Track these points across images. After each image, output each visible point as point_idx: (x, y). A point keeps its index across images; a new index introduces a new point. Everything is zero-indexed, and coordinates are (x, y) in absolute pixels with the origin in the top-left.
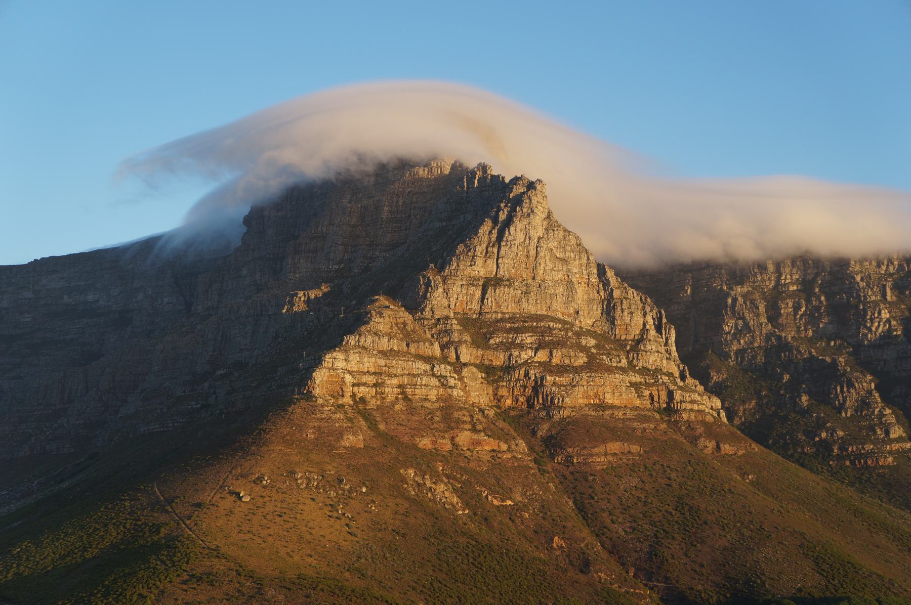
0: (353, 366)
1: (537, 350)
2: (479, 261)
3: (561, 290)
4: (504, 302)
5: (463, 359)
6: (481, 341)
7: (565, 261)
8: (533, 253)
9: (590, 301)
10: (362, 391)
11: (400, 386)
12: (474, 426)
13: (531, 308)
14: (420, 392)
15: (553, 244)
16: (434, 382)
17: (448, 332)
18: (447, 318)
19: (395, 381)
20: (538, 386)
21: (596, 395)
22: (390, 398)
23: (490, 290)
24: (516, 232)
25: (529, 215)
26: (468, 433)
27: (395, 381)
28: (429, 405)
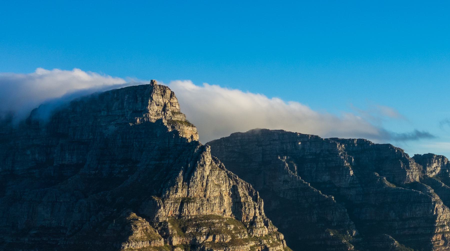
2: (180, 190)
3: (217, 200)
4: (191, 211)
7: (219, 186)
8: (205, 184)
13: (206, 212)
17: (166, 230)
18: (165, 222)
24: (198, 174)
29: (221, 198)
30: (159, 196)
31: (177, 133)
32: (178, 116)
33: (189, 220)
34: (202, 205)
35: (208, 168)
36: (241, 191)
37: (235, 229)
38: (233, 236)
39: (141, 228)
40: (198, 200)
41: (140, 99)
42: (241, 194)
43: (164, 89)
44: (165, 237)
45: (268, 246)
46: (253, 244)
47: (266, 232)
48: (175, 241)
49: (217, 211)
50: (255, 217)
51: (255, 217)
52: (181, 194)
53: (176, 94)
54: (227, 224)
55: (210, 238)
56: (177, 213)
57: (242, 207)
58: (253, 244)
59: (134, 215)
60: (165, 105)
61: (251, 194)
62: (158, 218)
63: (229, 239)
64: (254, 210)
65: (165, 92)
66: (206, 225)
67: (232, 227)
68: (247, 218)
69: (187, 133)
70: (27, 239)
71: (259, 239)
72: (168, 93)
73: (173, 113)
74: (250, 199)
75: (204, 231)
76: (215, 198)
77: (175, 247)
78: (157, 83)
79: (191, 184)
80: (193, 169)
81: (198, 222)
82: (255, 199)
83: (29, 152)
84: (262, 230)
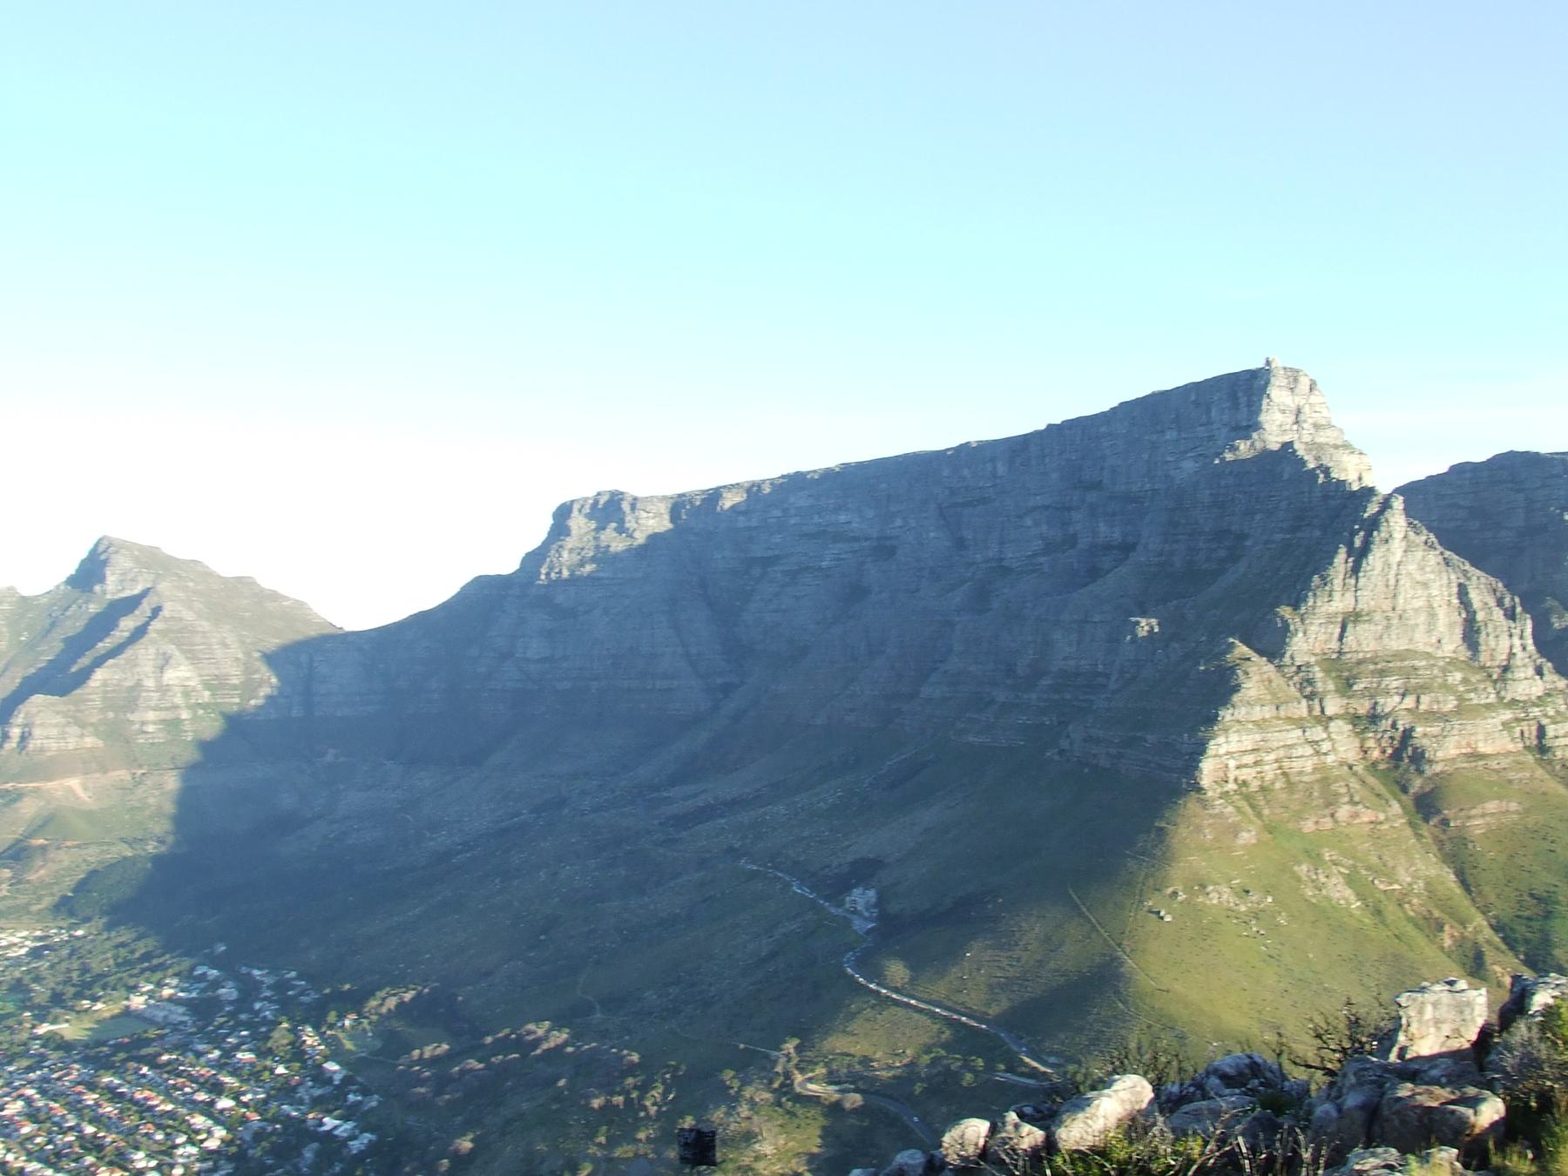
0: (1233, 747)
1: (1404, 695)
2: (1337, 596)
3: (1422, 618)
4: (1363, 640)
5: (1329, 711)
6: (1346, 686)
7: (1425, 585)
8: (1392, 582)
9: (1451, 625)
10: (1245, 774)
11: (1277, 761)
12: (1352, 797)
13: (1396, 643)
14: (1297, 765)
15: (1412, 567)
16: (1309, 750)
17: (1310, 682)
18: (1308, 665)
19: (1272, 756)
20: (1407, 734)
21: (1469, 745)
22: (1269, 776)
23: (1350, 627)
24: (1374, 560)
25: (1387, 541)
26: (1347, 807)
27: (1272, 756)
28: (1305, 779)
29: (1432, 615)
30: (1296, 607)
31: (1327, 471)
32: (1329, 432)
33: (1359, 662)
34: (1388, 627)
35: (1397, 546)
36: (1475, 597)
37: (1465, 681)
38: (1460, 699)
39: (1257, 678)
40: (1377, 617)
41: (1243, 400)
42: (1476, 604)
43: (1294, 376)
44: (1310, 697)
45: (1544, 721)
46: (1507, 715)
47: (1537, 688)
48: (1333, 706)
49: (1422, 642)
50: (1511, 655)
51: (1511, 655)
52: (1341, 603)
53: (1319, 386)
54: (1444, 671)
55: (1409, 702)
56: (1335, 645)
57: (1478, 631)
58: (1507, 715)
59: (1242, 649)
60: (1299, 412)
61: (1500, 603)
62: (1292, 658)
63: (1450, 704)
64: (1510, 639)
65: (1296, 380)
66: (1400, 671)
67: (1458, 676)
68: (1492, 658)
69: (1349, 471)
70: (1034, 696)
71: (1524, 705)
72: (1304, 384)
73: (1316, 426)
74: (1498, 614)
75: (1395, 684)
76: (1416, 610)
77: (1330, 718)
78: (1278, 363)
79: (1362, 581)
80: (1365, 551)
81: (1382, 666)
82: (1511, 615)
83: (1028, 522)
84: (1526, 685)
